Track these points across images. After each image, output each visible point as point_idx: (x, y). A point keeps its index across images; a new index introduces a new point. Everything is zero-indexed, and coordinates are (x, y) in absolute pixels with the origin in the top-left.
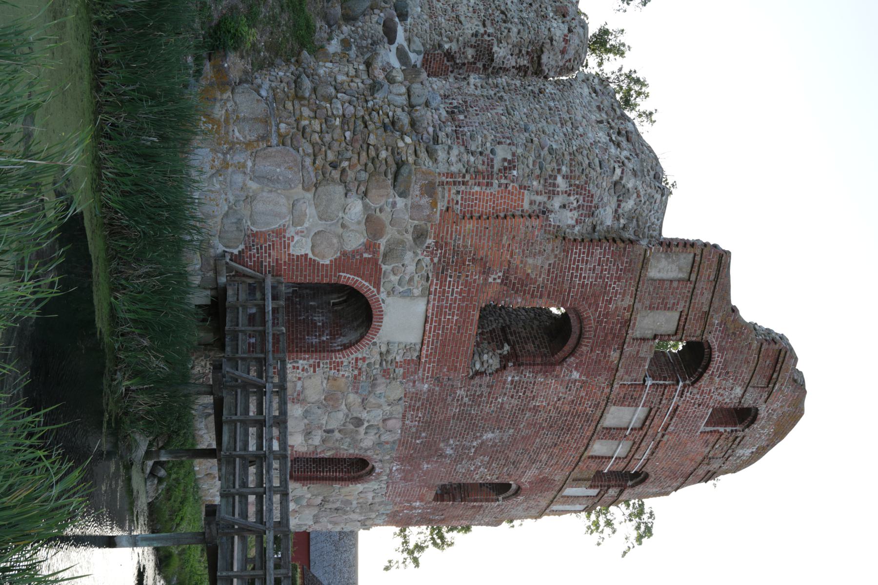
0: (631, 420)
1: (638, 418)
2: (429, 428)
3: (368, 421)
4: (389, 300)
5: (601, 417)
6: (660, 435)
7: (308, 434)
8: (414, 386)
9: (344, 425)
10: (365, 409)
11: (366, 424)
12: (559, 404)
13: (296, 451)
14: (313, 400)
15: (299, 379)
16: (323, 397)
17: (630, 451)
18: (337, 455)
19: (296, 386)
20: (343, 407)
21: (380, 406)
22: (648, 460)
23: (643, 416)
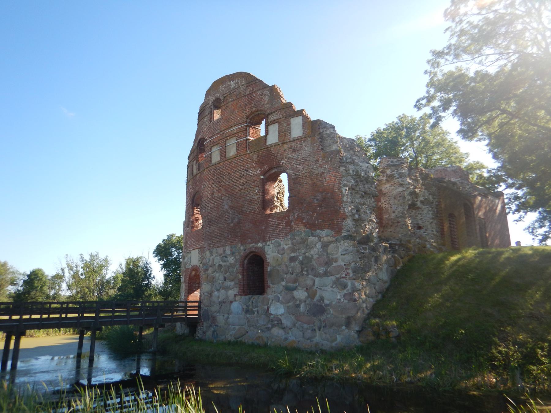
0: (217, 150)
1: (217, 148)
2: (222, 235)
3: (219, 262)
4: (191, 263)
5: (214, 165)
6: (222, 133)
7: (227, 289)
8: (205, 248)
9: (222, 272)
10: (215, 265)
11: (221, 263)
12: (210, 186)
13: (239, 293)
14: (210, 287)
15: (204, 294)
16: (210, 283)
17: (231, 138)
18: (241, 273)
19: (206, 295)
20: (213, 274)
21: (213, 259)
22: (235, 126)
23: (215, 147)
